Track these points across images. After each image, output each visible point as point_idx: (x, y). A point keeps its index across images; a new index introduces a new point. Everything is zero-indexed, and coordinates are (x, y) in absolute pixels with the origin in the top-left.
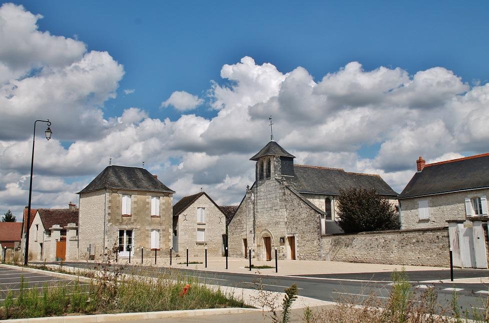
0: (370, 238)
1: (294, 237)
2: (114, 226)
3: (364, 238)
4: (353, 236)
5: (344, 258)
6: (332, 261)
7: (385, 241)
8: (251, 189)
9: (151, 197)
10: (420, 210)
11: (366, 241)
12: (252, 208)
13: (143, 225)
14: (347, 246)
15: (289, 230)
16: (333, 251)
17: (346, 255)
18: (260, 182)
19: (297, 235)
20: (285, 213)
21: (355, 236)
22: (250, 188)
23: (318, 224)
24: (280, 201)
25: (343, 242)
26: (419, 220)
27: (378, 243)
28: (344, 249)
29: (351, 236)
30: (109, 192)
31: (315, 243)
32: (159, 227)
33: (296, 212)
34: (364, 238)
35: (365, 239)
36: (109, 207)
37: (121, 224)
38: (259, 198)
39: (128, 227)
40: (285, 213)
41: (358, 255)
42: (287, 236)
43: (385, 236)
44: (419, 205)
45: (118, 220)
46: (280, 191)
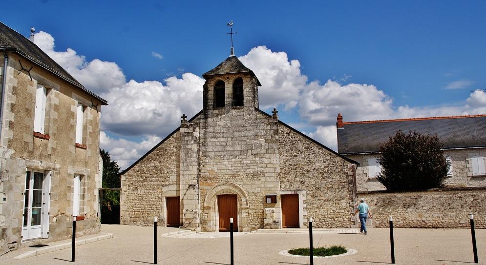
0: (449, 196)
1: (296, 196)
2: (18, 158)
3: (438, 196)
4: (419, 193)
5: (402, 222)
6: (377, 227)
7: (476, 200)
8: (190, 121)
9: (76, 102)
10: (369, 167)
11: (443, 200)
12: (196, 150)
13: (64, 163)
14: (406, 206)
15: (283, 186)
16: (380, 214)
17: (404, 219)
18: (216, 111)
19: (304, 192)
20: (276, 160)
21: (423, 194)
22: (188, 119)
23: (351, 178)
24: (266, 141)
25: (399, 202)
26: (369, 179)
27: (462, 202)
28: (400, 210)
29: (414, 194)
30: (14, 66)
31: (343, 203)
32: (84, 169)
33: (301, 160)
34: (438, 196)
35: (440, 197)
36: (12, 105)
37: (31, 153)
38: (210, 135)
39: (39, 165)
40: (276, 160)
41: (427, 218)
42: (279, 193)
43: (475, 193)
44: (369, 163)
45: (27, 143)
46: (268, 128)
